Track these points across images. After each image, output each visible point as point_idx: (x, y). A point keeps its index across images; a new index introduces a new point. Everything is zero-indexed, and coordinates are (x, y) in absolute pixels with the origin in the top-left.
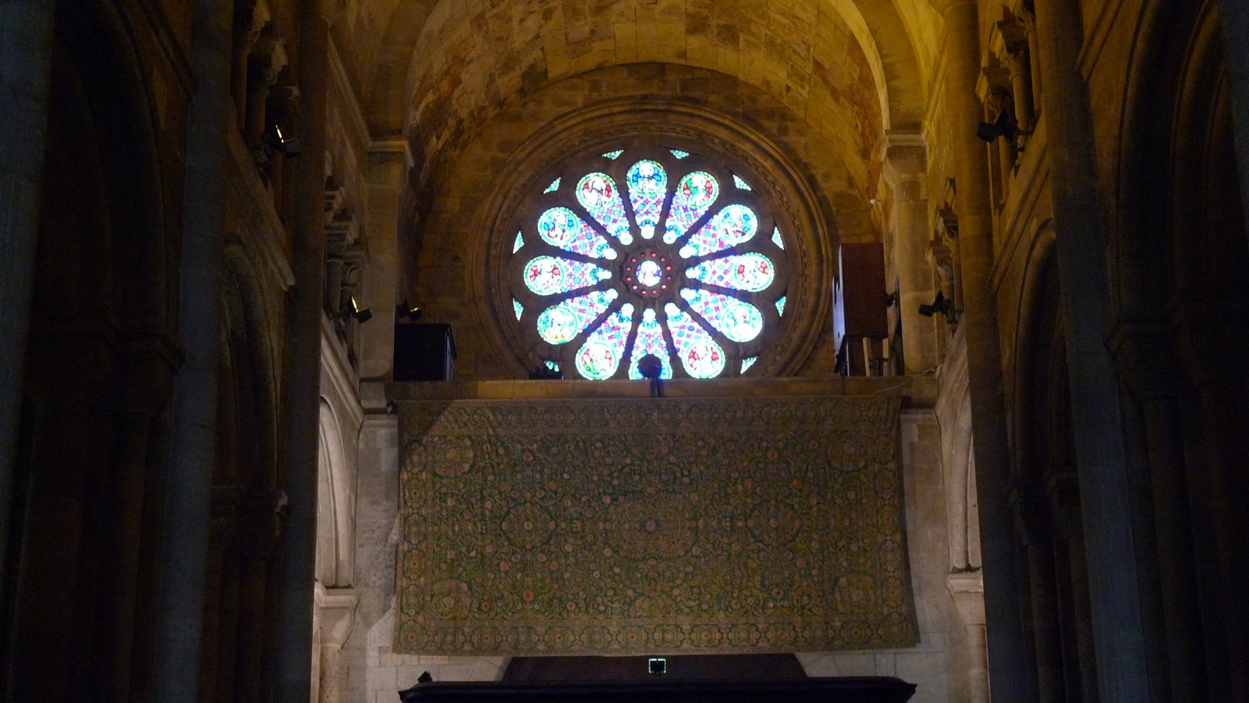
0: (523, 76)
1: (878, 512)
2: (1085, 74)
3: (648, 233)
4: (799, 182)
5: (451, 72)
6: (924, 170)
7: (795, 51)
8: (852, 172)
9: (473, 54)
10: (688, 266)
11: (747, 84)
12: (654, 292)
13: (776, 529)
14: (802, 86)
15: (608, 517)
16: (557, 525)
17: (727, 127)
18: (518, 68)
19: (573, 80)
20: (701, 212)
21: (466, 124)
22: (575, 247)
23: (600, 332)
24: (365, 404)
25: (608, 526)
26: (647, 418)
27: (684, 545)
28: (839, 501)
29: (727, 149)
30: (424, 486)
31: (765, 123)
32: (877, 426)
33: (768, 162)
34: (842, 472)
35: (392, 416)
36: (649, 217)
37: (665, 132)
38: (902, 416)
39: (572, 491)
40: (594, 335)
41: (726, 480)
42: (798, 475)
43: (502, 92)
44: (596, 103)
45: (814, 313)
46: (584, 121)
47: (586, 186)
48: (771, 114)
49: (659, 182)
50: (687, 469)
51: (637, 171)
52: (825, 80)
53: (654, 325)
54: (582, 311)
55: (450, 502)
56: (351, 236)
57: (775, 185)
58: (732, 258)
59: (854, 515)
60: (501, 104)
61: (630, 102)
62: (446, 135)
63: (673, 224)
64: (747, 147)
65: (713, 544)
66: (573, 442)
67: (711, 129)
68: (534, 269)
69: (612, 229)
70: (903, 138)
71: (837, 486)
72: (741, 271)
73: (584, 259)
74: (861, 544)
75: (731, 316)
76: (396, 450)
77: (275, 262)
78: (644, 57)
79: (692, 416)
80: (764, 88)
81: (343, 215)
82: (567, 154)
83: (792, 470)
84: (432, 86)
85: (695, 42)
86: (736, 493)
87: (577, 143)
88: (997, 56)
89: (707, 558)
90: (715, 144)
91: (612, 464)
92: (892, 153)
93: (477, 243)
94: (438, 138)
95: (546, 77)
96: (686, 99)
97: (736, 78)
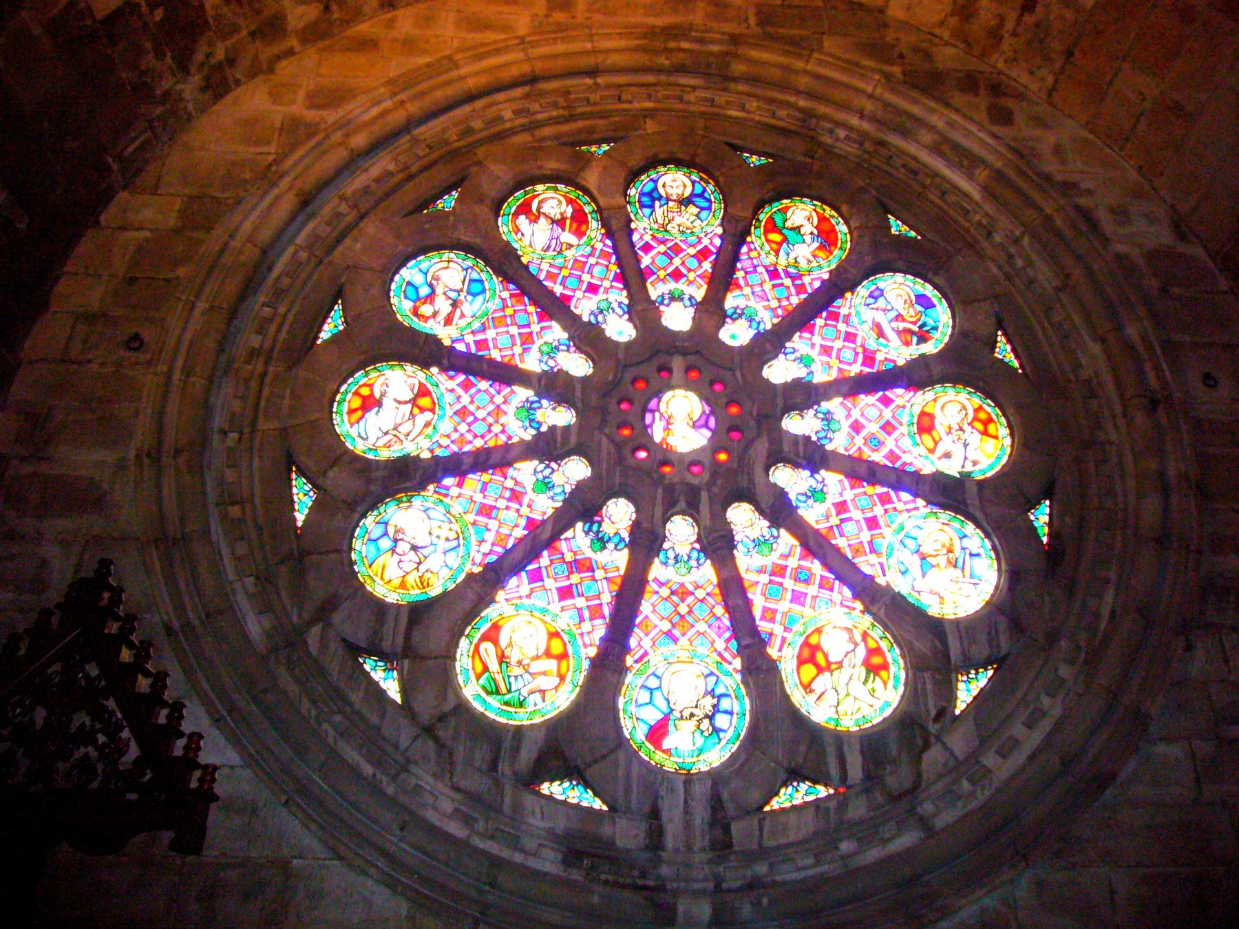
3: (678, 319)
10: (788, 409)
12: (695, 469)
20: (812, 282)
22: (481, 344)
23: (536, 576)
36: (681, 285)
40: (518, 585)
49: (704, 214)
51: (651, 185)
53: (693, 563)
54: (487, 511)
58: (898, 394)
63: (742, 303)
68: (365, 391)
69: (584, 307)
73: (505, 374)
87: (508, 114)
90: (837, 139)
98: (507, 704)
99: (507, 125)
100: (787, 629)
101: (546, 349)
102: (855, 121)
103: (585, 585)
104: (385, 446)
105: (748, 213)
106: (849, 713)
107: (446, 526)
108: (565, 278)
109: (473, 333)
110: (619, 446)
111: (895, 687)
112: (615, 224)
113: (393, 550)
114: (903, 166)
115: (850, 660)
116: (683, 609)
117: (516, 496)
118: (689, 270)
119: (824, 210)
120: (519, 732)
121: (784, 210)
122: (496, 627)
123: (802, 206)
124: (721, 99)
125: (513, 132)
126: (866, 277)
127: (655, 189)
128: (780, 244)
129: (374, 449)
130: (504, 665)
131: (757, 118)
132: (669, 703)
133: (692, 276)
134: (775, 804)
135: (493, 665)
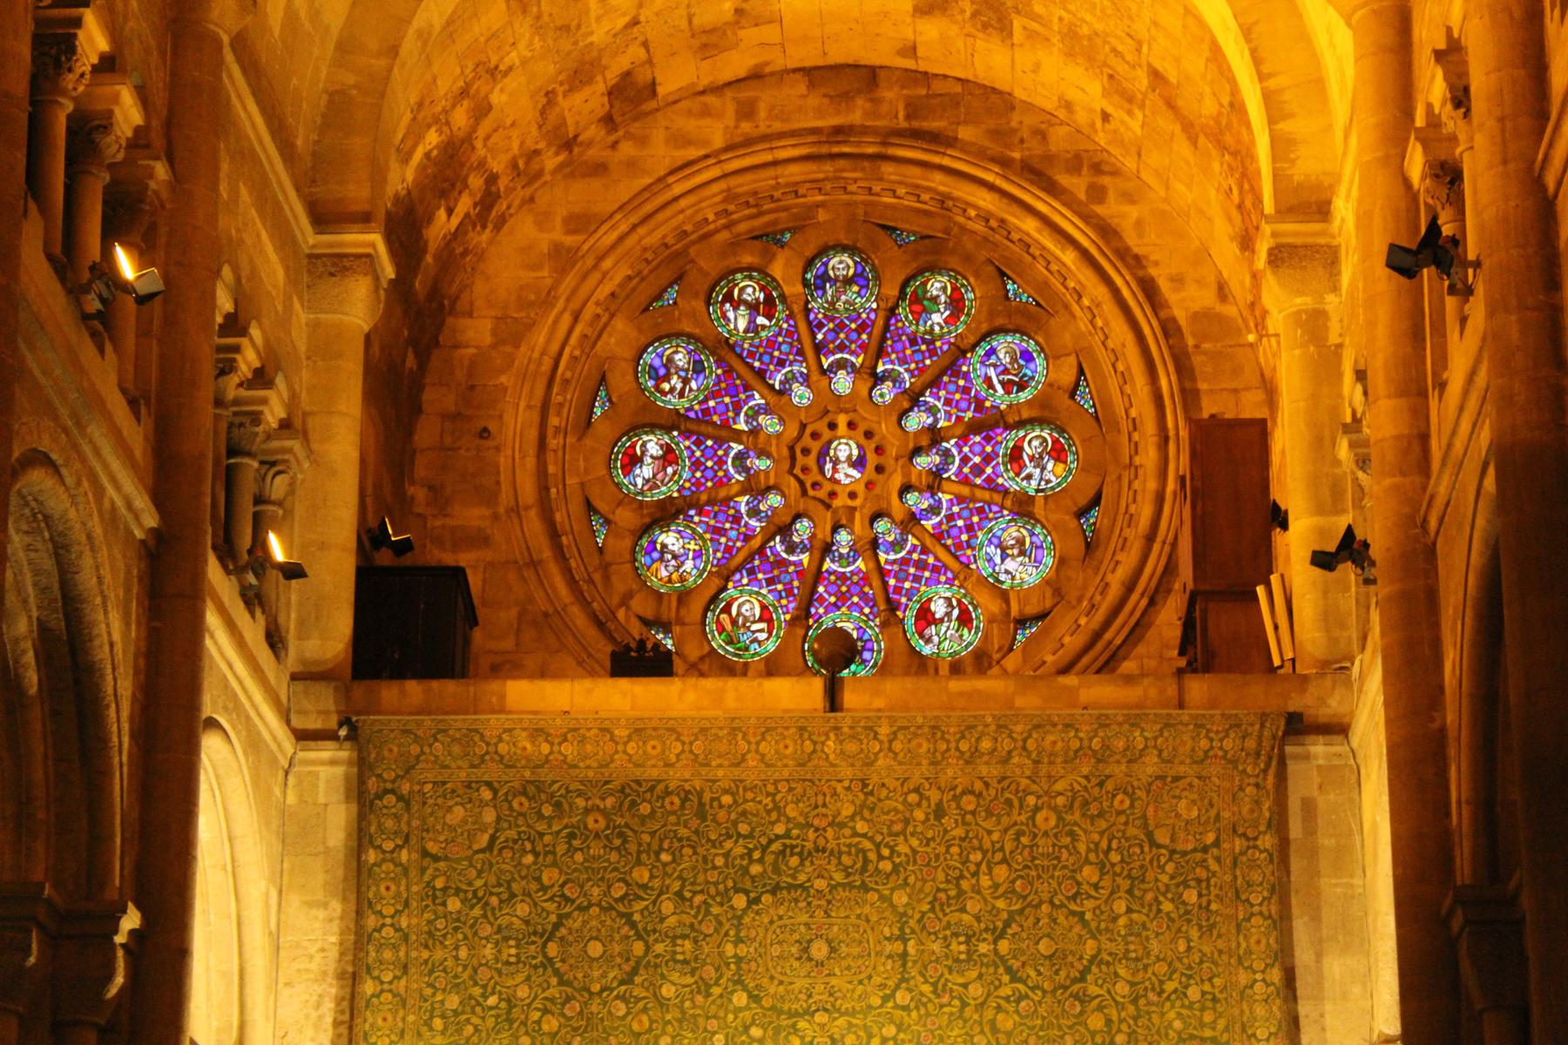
0: (610, 93)
1: (1238, 926)
2: (1550, 182)
4: (1126, 293)
5: (472, 92)
6: (1335, 289)
7: (1114, 50)
8: (1225, 274)
9: (513, 57)
11: (1029, 107)
13: (1050, 957)
14: (1130, 113)
15: (742, 934)
16: (648, 948)
17: (991, 187)
18: (599, 78)
19: (702, 98)
21: (503, 183)
23: (752, 572)
24: (297, 723)
25: (742, 950)
26: (814, 751)
27: (882, 986)
28: (1167, 906)
29: (992, 229)
30: (406, 871)
31: (1064, 180)
32: (1241, 768)
33: (1068, 253)
34: (1173, 852)
35: (347, 744)
37: (878, 195)
38: (1289, 749)
39: (676, 886)
41: (958, 865)
42: (1092, 857)
43: (570, 121)
44: (748, 142)
45: (1150, 538)
46: (725, 176)
47: (728, 297)
48: (1075, 164)
50: (887, 845)
51: (823, 269)
52: (1171, 105)
54: (721, 532)
55: (454, 904)
56: (274, 413)
57: (1080, 297)
59: (1194, 934)
60: (568, 144)
61: (811, 139)
62: (464, 205)
64: (1030, 225)
65: (935, 985)
66: (678, 795)
67: (964, 191)
70: (1295, 230)
71: (1165, 879)
72: (1016, 455)
74: (1207, 987)
75: (995, 541)
76: (354, 807)
77: (118, 488)
78: (837, 56)
79: (897, 746)
80: (1062, 114)
81: (261, 378)
82: (694, 237)
83: (1082, 848)
84: (436, 120)
85: (930, 31)
86: (977, 890)
87: (711, 217)
88: (1437, 111)
89: (923, 1011)
90: (969, 219)
91: (750, 836)
92: (1277, 257)
93: (523, 404)
94: (450, 212)
95: (654, 93)
96: (916, 134)
97: (1010, 94)
98: (739, 649)
101: (750, 413)
108: (761, 355)
109: (699, 403)
110: (802, 483)
111: (976, 633)
113: (661, 559)
116: (844, 589)
117: (737, 519)
118: (851, 342)
119: (957, 280)
121: (924, 284)
123: (940, 278)
127: (826, 272)
128: (920, 314)
129: (642, 492)
133: (853, 346)
135: (728, 626)
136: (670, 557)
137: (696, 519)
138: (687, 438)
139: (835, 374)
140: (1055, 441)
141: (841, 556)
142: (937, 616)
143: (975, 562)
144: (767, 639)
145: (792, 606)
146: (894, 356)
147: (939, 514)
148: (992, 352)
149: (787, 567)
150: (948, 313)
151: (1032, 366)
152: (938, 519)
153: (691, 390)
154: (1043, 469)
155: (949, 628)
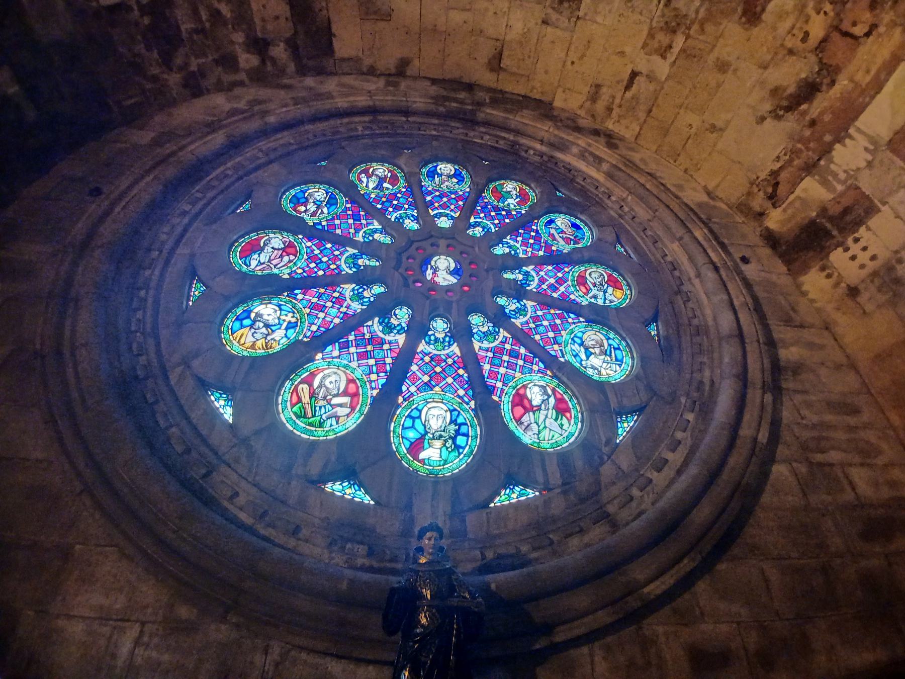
3: (444, 223)
23: (345, 346)
37: (470, 137)
40: (333, 350)
51: (434, 168)
53: (447, 344)
72: (581, 281)
87: (360, 128)
90: (530, 155)
98: (310, 424)
99: (360, 133)
100: (505, 384)
101: (368, 232)
102: (538, 146)
103: (375, 352)
104: (260, 270)
105: (484, 181)
106: (546, 439)
107: (291, 315)
109: (327, 220)
110: (405, 279)
111: (576, 424)
112: (412, 180)
114: (563, 166)
115: (546, 406)
117: (339, 301)
118: (451, 204)
120: (313, 445)
122: (313, 375)
124: (471, 134)
125: (363, 137)
126: (546, 214)
127: (436, 170)
129: (253, 271)
130: (313, 399)
131: (489, 143)
132: (425, 428)
134: (497, 502)
135: (306, 399)
136: (261, 325)
137: (300, 297)
138: (309, 241)
139: (439, 218)
140: (610, 276)
141: (436, 340)
142: (535, 403)
143: (564, 357)
144: (348, 415)
145: (382, 381)
146: (482, 215)
147: (526, 315)
148: (551, 222)
149: (382, 344)
150: (518, 199)
151: (580, 231)
152: (525, 319)
153: (322, 213)
154: (605, 292)
155: (547, 416)
